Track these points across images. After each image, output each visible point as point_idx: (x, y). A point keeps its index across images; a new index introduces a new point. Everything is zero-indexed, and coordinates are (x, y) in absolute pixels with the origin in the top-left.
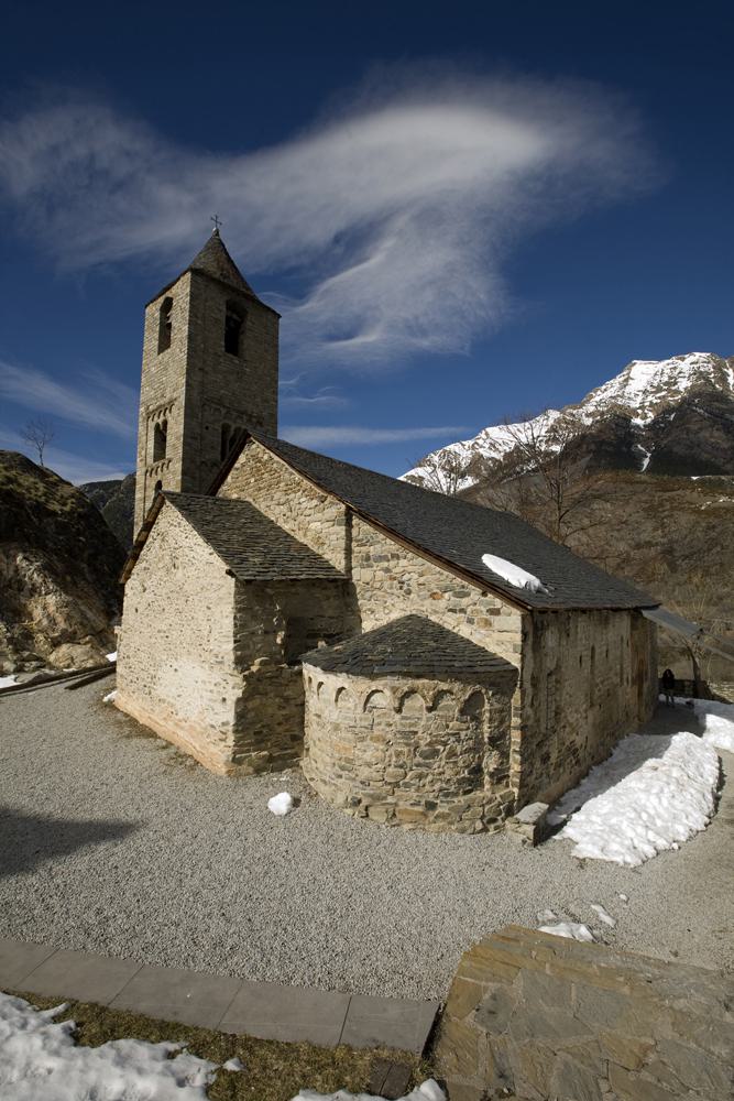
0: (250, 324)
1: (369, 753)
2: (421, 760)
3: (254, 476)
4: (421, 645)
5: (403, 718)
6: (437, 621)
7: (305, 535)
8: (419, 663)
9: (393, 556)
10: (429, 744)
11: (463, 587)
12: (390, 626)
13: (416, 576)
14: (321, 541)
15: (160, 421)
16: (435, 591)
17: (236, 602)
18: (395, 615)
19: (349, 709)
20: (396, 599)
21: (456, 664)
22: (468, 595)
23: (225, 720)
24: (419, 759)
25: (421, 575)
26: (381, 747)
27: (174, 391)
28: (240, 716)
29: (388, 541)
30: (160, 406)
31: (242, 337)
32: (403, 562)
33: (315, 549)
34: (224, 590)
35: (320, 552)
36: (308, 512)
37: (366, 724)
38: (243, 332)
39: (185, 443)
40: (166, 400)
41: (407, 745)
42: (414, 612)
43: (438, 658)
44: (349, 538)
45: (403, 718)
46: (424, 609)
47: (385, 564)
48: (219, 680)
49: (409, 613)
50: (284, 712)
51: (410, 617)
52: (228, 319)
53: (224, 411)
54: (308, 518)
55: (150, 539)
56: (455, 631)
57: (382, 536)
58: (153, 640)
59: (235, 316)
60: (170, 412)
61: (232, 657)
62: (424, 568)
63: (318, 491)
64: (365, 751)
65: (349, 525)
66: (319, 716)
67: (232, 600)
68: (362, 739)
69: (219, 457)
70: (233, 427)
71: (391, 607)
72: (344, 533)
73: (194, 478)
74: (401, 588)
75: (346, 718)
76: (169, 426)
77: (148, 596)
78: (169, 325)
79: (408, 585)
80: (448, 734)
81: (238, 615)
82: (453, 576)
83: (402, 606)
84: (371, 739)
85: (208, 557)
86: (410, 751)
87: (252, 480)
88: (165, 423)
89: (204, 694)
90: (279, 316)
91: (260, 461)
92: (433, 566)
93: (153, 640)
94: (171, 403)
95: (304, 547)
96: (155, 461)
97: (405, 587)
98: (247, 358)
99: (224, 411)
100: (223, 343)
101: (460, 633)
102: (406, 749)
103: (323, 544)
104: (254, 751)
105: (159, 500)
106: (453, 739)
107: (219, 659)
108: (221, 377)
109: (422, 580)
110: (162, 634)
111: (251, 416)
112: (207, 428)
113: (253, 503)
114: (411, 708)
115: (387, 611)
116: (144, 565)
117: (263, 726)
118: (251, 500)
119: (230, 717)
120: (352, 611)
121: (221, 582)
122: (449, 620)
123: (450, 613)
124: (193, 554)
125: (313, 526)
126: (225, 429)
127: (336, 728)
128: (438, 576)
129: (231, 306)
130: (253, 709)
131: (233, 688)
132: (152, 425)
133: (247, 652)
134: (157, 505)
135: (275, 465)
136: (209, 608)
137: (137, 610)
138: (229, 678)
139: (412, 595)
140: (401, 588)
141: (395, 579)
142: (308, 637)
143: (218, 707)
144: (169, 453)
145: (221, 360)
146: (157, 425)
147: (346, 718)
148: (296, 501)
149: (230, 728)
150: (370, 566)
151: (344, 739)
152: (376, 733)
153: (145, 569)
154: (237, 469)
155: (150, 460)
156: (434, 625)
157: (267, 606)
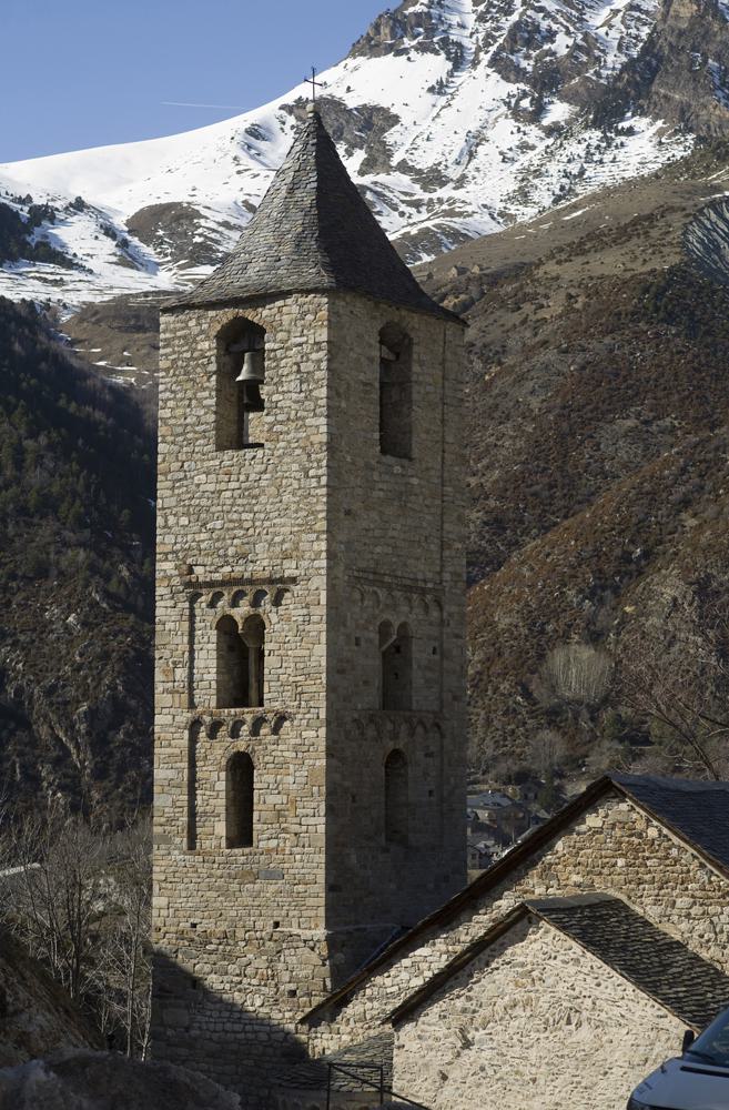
3: (624, 856)
15: (241, 612)
30: (239, 581)
39: (331, 689)
40: (261, 566)
87: (621, 862)
88: (257, 625)
91: (640, 836)
94: (280, 587)
108: (374, 515)
111: (423, 592)
116: (459, 1003)
118: (624, 898)
126: (384, 629)
144: (275, 696)
155: (207, 697)
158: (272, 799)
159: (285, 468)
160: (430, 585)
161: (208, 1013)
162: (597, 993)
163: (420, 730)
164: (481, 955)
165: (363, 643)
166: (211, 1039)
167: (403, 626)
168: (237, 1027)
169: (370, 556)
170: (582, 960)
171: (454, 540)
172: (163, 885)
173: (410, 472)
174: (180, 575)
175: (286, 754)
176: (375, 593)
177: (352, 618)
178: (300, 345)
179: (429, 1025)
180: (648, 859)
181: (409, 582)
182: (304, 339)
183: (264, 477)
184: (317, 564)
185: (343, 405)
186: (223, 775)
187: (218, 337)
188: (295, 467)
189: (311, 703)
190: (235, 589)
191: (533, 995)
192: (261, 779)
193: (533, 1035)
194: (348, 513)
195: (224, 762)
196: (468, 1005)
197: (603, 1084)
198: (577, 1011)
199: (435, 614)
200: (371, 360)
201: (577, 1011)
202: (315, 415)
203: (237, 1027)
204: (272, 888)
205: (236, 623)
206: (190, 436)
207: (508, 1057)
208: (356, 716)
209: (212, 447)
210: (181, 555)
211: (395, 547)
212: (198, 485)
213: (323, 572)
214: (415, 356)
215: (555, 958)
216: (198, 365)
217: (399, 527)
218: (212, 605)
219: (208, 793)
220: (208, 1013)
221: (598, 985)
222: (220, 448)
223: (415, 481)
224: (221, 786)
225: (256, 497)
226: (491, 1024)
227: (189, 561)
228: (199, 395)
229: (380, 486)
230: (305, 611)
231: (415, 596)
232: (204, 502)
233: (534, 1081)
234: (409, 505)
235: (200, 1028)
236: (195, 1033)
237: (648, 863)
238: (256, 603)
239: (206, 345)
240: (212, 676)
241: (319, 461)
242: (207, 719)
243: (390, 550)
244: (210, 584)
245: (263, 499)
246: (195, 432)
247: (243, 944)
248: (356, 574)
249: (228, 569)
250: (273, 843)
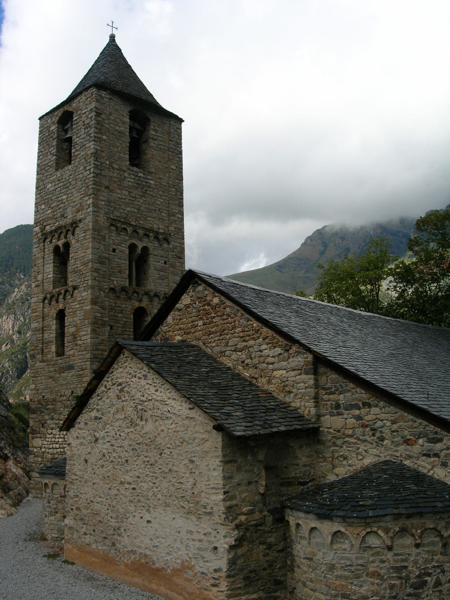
0: (154, 133)
1: (365, 588)
2: (409, 590)
3: (201, 319)
4: (405, 489)
5: (396, 555)
6: (411, 465)
7: (269, 382)
8: (408, 505)
9: (364, 404)
10: (419, 576)
11: (436, 433)
12: (366, 470)
13: (389, 424)
14: (287, 389)
15: (60, 243)
16: (409, 437)
17: (224, 456)
18: (368, 461)
19: (345, 550)
20: (369, 445)
21: (439, 505)
22: (440, 440)
23: (217, 568)
24: (409, 590)
25: (394, 422)
26: (377, 581)
27: (78, 211)
28: (232, 563)
29: (358, 390)
30: (60, 228)
31: (144, 146)
32: (375, 410)
33: (281, 397)
34: (208, 445)
35: (287, 399)
36: (270, 360)
37: (360, 562)
38: (146, 141)
40: (68, 220)
41: (400, 578)
42: (388, 458)
43: (421, 501)
44: (317, 386)
45: (396, 555)
46: (398, 454)
47: (357, 412)
48: (209, 530)
49: (383, 459)
50: (267, 558)
51: (386, 463)
52: (131, 128)
54: (271, 366)
55: (101, 389)
56: (430, 474)
57: (351, 385)
58: (114, 492)
59: (137, 126)
60: (73, 234)
61: (223, 509)
62: (397, 416)
63: (281, 340)
64: (361, 586)
65: (315, 373)
66: (310, 559)
67: (220, 453)
68: (357, 577)
69: (127, 284)
70: (140, 246)
71: (364, 453)
72: (312, 382)
73: (103, 308)
74: (374, 435)
75: (342, 558)
76: (71, 250)
77: (102, 447)
78: (69, 140)
79: (381, 432)
80: (434, 567)
81: (226, 467)
82: (425, 423)
83: (375, 452)
84: (367, 575)
85: (188, 412)
86: (402, 583)
87: (200, 323)
88: (67, 245)
89: (191, 543)
90: (181, 121)
91: (209, 305)
92: (406, 414)
93: (114, 492)
94: (74, 224)
95: (269, 395)
96: (54, 288)
97: (378, 435)
98: (153, 170)
99: (130, 230)
100: (127, 156)
101: (435, 476)
102: (398, 582)
103: (290, 392)
104: (244, 594)
105: (115, 350)
106: (438, 571)
107: (209, 510)
108: (126, 193)
109: (395, 427)
110: (127, 486)
111: (157, 233)
112: (114, 250)
113: (203, 347)
114: (403, 546)
115: (360, 457)
116: (94, 414)
117: (250, 572)
119: (223, 563)
120: (324, 457)
121: (205, 436)
122: (423, 463)
123: (424, 458)
124: (166, 408)
125: (277, 373)
126: (132, 248)
127: (332, 568)
128: (411, 423)
129: (133, 116)
130: (242, 555)
131: (225, 537)
132: (49, 248)
133: (234, 502)
134: (113, 355)
135: (228, 310)
136: (192, 462)
137: (86, 461)
138: (221, 529)
139: (386, 442)
140: (374, 435)
141: (367, 426)
142: (282, 485)
143: (209, 555)
144: (72, 279)
145: (126, 175)
146: (57, 248)
147: (342, 558)
148: (256, 348)
149: (223, 574)
150: (339, 414)
151: (341, 577)
152: (371, 569)
153: (96, 418)
154: (180, 310)
155: (49, 287)
156: (409, 469)
157: (249, 457)
158: (72, 330)
159: (79, 170)
160: (161, 231)
161: (47, 440)
162: (155, 397)
163: (157, 299)
164: (102, 382)
165: (117, 251)
166: (48, 453)
167: (145, 249)
168: (58, 446)
169: (122, 211)
170: (148, 375)
171: (176, 213)
172: (34, 379)
173: (149, 177)
174: (41, 232)
175: (77, 306)
176: (125, 229)
177: (110, 238)
178: (85, 113)
179: (81, 429)
180: (214, 317)
181: (148, 228)
182: (86, 110)
183: (71, 177)
184: (89, 210)
185: (104, 137)
186: (54, 322)
187: (58, 123)
188: (82, 168)
189: (86, 279)
190: (59, 232)
191: (125, 403)
192: (68, 320)
193: (127, 430)
194: (107, 188)
195: (55, 315)
196: (97, 414)
197: (160, 462)
198: (145, 411)
199: (166, 245)
200: (124, 123)
201: (145, 411)
202: (90, 142)
203: (58, 446)
204: (70, 374)
205: (60, 248)
206: (46, 168)
207: (115, 447)
208: (112, 286)
209: (54, 170)
210: (42, 222)
211: (139, 210)
212: (48, 189)
213: (91, 213)
214: (152, 127)
215: (135, 377)
216: (50, 137)
217: (142, 201)
218: (51, 242)
219: (49, 332)
220: (47, 440)
221: (157, 391)
222: (57, 170)
223: (152, 182)
224: (54, 327)
225: (68, 187)
226: (108, 426)
227: (45, 224)
228: (50, 150)
229: (129, 180)
230: (84, 234)
231: (151, 234)
232: (50, 196)
233: (127, 461)
234: (148, 192)
235: (45, 447)
236: (43, 450)
237: (214, 320)
238: (66, 237)
239: (53, 128)
240: (51, 276)
241: (90, 162)
242: (48, 296)
243: (136, 211)
244: (51, 232)
245: (70, 187)
246: (48, 166)
247: (59, 403)
248: (112, 217)
249: (57, 223)
250: (71, 352)
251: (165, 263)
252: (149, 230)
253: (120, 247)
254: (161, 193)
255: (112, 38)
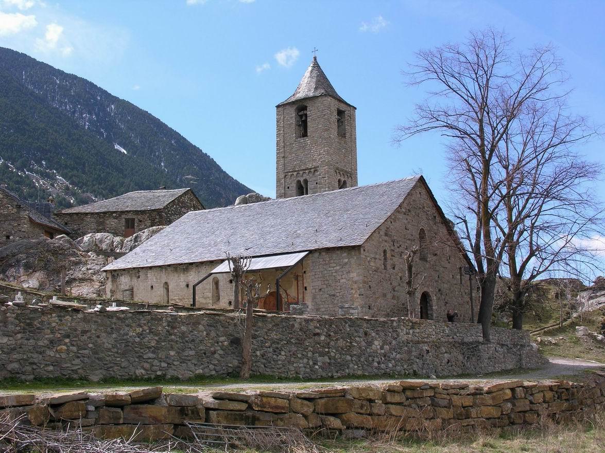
0: (309, 113)
53: (295, 174)
70: (302, 180)
108: (294, 155)
112: (288, 188)
251: (317, 183)
252: (306, 170)
253: (291, 185)
254: (314, 145)
255: (315, 58)
